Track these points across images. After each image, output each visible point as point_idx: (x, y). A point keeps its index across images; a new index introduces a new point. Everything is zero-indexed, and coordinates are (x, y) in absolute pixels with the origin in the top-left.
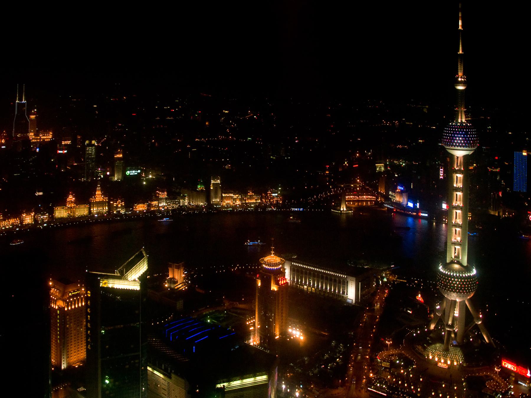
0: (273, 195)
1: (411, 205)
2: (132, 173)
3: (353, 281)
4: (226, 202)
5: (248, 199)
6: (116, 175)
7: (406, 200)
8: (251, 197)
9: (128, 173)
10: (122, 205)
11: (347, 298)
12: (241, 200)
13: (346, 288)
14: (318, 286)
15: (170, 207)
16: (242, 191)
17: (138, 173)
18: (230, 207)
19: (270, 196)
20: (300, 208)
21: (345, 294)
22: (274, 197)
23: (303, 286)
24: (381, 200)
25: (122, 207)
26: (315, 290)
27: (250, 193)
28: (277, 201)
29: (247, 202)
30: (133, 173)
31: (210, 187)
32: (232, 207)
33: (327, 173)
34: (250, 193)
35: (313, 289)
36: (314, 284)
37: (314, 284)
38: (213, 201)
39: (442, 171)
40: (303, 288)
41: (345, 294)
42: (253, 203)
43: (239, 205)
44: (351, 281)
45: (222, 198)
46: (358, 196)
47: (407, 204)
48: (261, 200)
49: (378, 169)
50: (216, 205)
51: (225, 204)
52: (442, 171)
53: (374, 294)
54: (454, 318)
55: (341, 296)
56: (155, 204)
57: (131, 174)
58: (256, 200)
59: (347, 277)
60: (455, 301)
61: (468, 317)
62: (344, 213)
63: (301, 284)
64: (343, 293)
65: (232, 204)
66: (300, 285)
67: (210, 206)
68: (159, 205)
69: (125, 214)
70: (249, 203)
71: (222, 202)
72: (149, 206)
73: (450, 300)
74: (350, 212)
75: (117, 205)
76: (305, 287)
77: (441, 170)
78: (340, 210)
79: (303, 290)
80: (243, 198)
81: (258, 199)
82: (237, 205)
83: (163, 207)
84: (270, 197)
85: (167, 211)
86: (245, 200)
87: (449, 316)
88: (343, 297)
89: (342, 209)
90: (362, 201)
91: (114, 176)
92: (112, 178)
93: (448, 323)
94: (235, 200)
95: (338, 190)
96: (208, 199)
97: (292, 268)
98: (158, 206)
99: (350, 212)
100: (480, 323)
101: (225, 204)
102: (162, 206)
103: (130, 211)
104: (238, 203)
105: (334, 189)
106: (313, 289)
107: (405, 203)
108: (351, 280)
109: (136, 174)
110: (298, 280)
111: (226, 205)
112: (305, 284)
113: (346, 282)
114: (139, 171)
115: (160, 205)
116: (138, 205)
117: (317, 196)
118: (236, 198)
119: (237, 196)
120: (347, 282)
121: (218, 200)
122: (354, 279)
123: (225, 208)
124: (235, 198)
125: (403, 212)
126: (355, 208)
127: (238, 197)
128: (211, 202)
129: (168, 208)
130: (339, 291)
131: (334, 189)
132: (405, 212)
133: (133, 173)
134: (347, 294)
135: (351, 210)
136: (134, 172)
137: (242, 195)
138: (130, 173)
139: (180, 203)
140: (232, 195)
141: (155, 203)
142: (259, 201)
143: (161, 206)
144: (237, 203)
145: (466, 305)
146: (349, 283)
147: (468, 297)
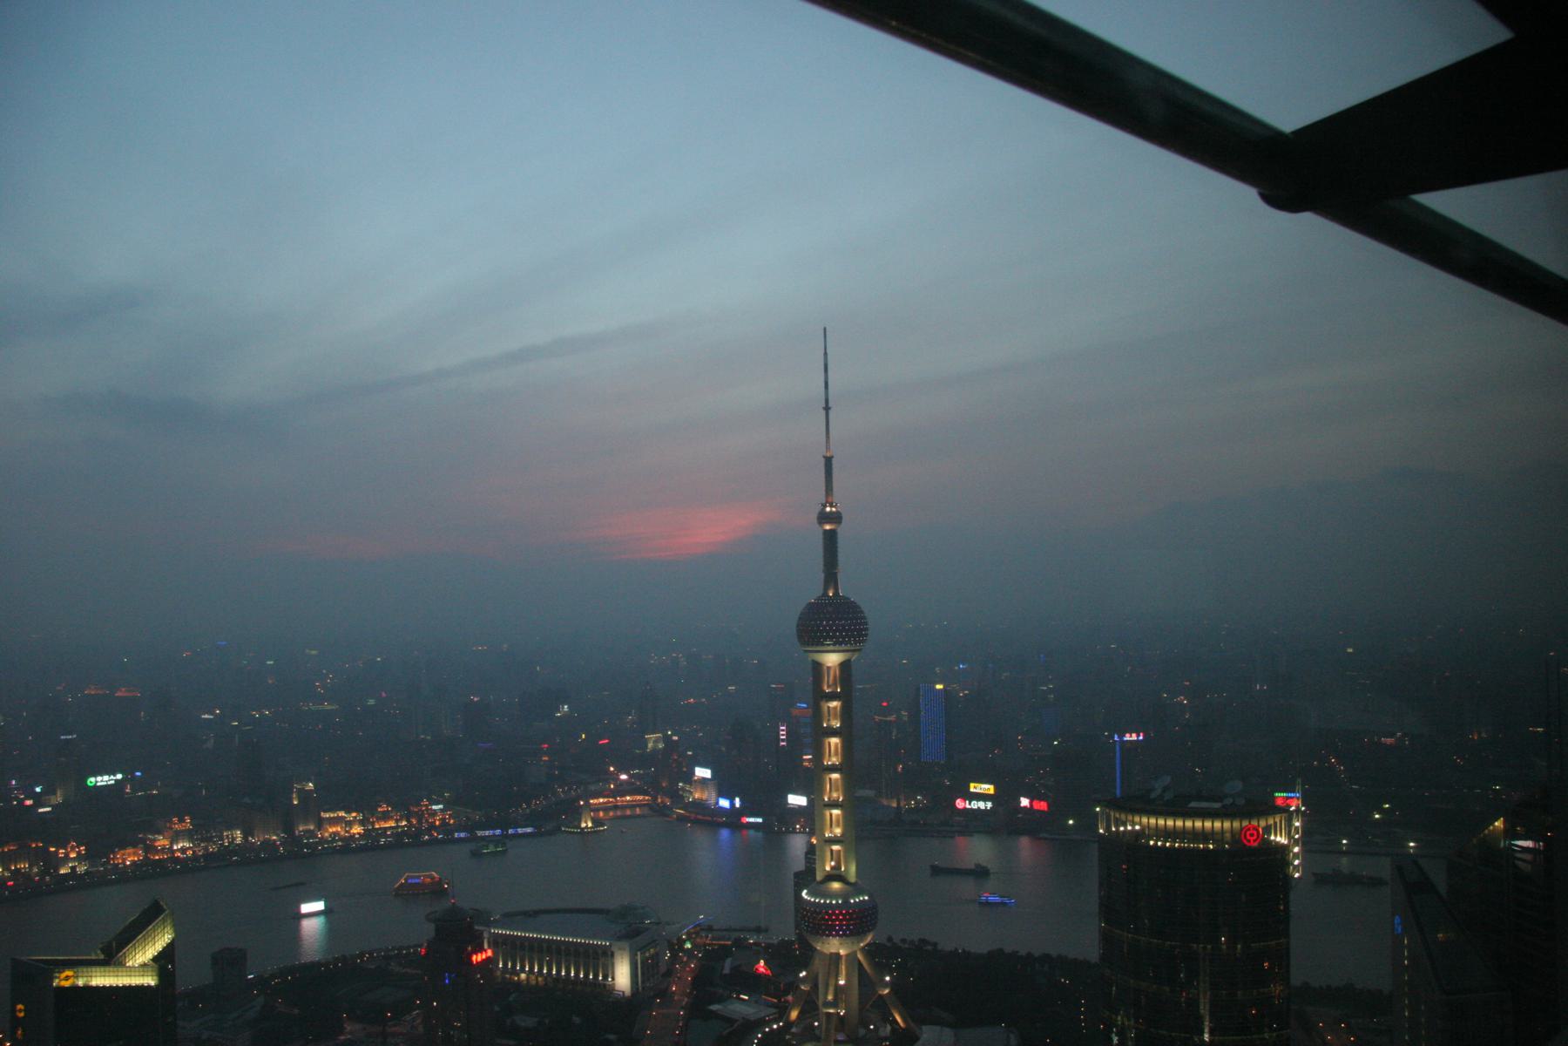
0: (434, 807)
1: (724, 803)
2: (102, 781)
3: (624, 949)
4: (331, 830)
5: (379, 819)
6: (59, 793)
7: (714, 795)
8: (385, 817)
9: (91, 782)
10: (79, 853)
11: (612, 987)
12: (362, 823)
13: (610, 968)
14: (550, 970)
15: (200, 851)
16: (365, 806)
17: (116, 780)
18: (340, 840)
19: (427, 809)
20: (494, 828)
21: (610, 979)
22: (434, 813)
23: (518, 975)
24: (662, 802)
25: (80, 858)
26: (546, 978)
27: (384, 808)
28: (443, 820)
29: (377, 826)
30: (104, 780)
31: (291, 799)
32: (342, 839)
33: (545, 761)
34: (384, 808)
35: (540, 979)
36: (541, 969)
37: (541, 969)
38: (301, 829)
39: (783, 730)
40: (519, 978)
41: (610, 979)
42: (391, 828)
43: (359, 834)
44: (620, 952)
45: (320, 823)
46: (616, 799)
47: (717, 803)
48: (408, 821)
49: (650, 745)
50: (308, 839)
51: (327, 834)
52: (783, 730)
53: (669, 973)
54: (838, 988)
55: (600, 985)
56: (164, 845)
57: (99, 784)
58: (397, 821)
59: (610, 945)
60: (838, 955)
61: (865, 982)
62: (588, 833)
63: (515, 972)
64: (606, 977)
65: (342, 833)
66: (511, 974)
67: (292, 840)
68: (171, 847)
69: (87, 873)
70: (380, 828)
71: (319, 830)
72: (150, 849)
73: (825, 954)
74: (602, 828)
75: (67, 855)
76: (523, 976)
77: (782, 728)
78: (579, 827)
79: (519, 982)
80: (368, 820)
81: (401, 820)
82: (354, 834)
83: (183, 850)
84: (428, 814)
85: (195, 858)
86: (373, 823)
87: (827, 986)
88: (605, 985)
89: (583, 825)
90: (623, 807)
91: (54, 793)
92: (50, 800)
93: (827, 999)
94: (350, 824)
95: (570, 789)
96: (289, 828)
97: (491, 939)
98: (173, 852)
99: (602, 828)
100: (887, 991)
101: (327, 834)
102: (182, 847)
103: (102, 865)
104: (357, 830)
105: (563, 789)
106: (540, 979)
107: (712, 801)
108: (620, 949)
109: (113, 782)
110: (505, 964)
111: (330, 835)
112: (523, 970)
113: (609, 953)
114: (119, 776)
115: (175, 848)
116: (122, 852)
117: (529, 806)
118: (353, 821)
119: (354, 814)
120: (612, 955)
121: (312, 827)
122: (625, 944)
123: (327, 842)
124: (350, 821)
125: (710, 819)
126: (611, 819)
127: (355, 817)
128: (294, 833)
129: (194, 852)
130: (596, 976)
131: (563, 789)
132: (715, 819)
133: (104, 780)
134: (613, 979)
135: (602, 825)
136: (106, 778)
137: (366, 812)
138: (97, 782)
139: (223, 840)
140: (342, 814)
141: (162, 842)
142: (404, 823)
143: (178, 850)
144: (355, 831)
145: (859, 961)
146: (616, 954)
147: (862, 945)
